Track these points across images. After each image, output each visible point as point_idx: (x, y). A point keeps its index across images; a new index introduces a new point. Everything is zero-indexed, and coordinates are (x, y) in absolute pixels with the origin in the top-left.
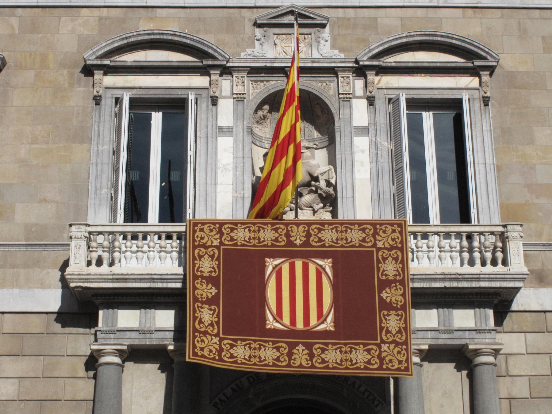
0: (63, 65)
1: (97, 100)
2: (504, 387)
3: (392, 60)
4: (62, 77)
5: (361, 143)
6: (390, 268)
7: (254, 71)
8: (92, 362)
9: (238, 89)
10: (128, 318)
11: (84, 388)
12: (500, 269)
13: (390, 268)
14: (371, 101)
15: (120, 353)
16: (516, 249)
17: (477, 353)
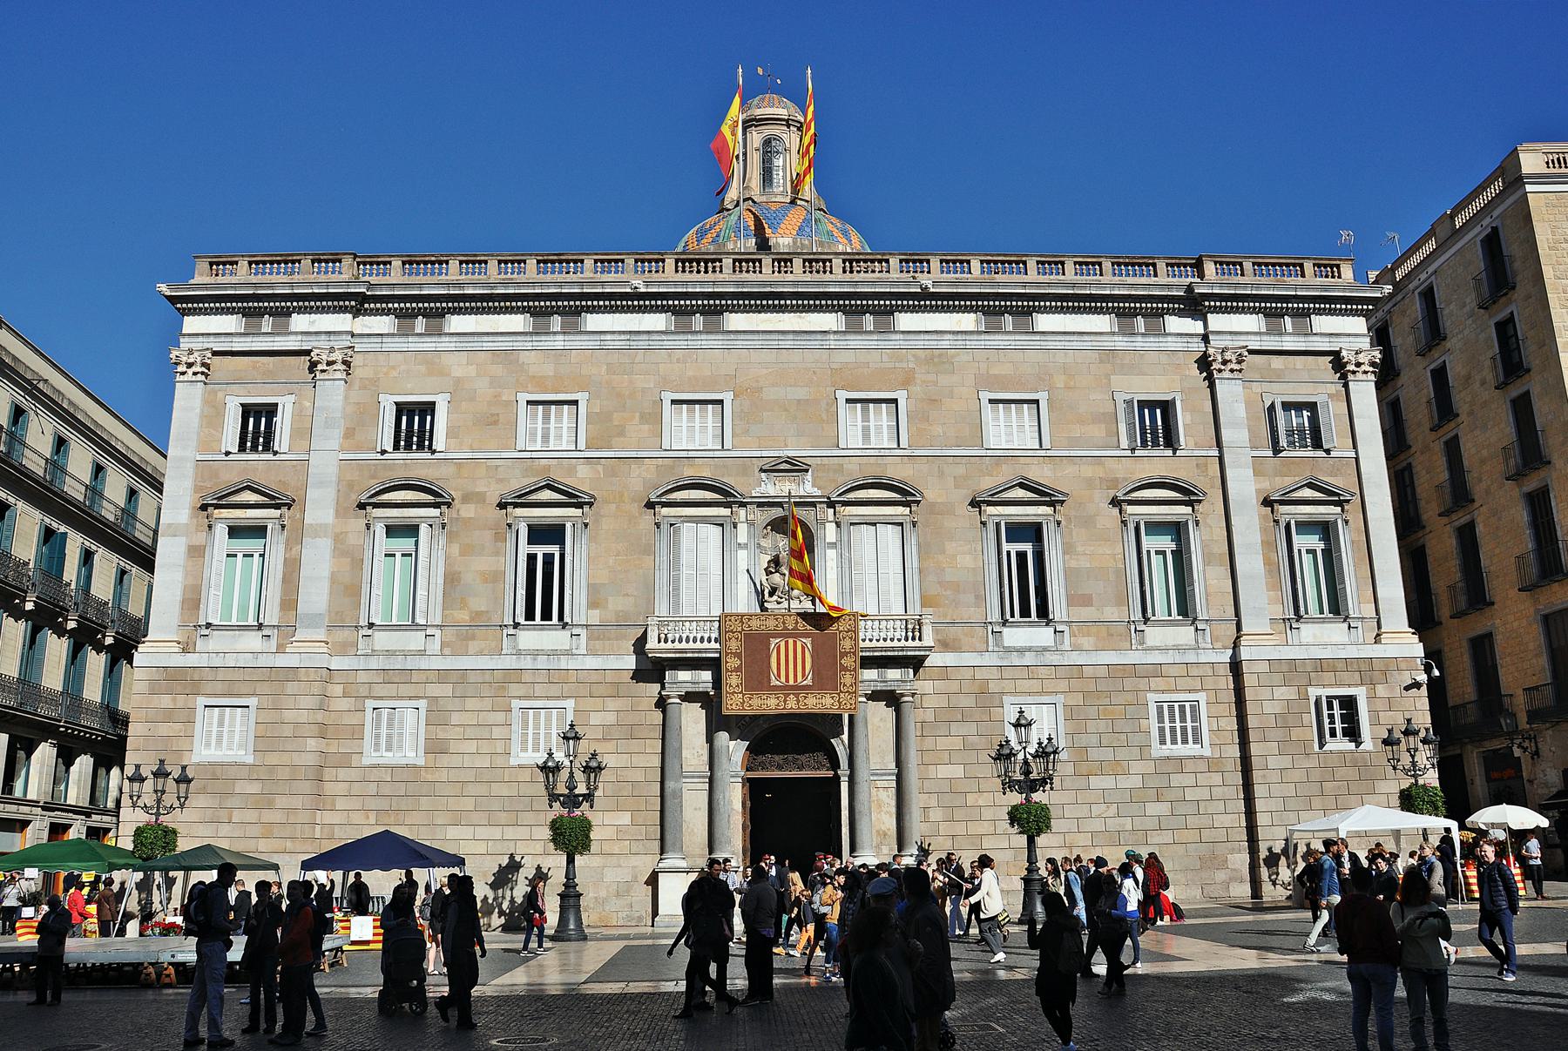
0: (633, 500)
1: (658, 525)
2: (920, 715)
3: (852, 496)
4: (636, 508)
5: (831, 554)
6: (847, 644)
7: (760, 505)
8: (662, 703)
9: (751, 517)
10: (684, 675)
11: (657, 716)
12: (917, 643)
13: (847, 644)
14: (838, 525)
15: (680, 697)
16: (928, 631)
17: (902, 695)
